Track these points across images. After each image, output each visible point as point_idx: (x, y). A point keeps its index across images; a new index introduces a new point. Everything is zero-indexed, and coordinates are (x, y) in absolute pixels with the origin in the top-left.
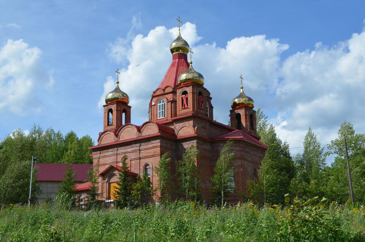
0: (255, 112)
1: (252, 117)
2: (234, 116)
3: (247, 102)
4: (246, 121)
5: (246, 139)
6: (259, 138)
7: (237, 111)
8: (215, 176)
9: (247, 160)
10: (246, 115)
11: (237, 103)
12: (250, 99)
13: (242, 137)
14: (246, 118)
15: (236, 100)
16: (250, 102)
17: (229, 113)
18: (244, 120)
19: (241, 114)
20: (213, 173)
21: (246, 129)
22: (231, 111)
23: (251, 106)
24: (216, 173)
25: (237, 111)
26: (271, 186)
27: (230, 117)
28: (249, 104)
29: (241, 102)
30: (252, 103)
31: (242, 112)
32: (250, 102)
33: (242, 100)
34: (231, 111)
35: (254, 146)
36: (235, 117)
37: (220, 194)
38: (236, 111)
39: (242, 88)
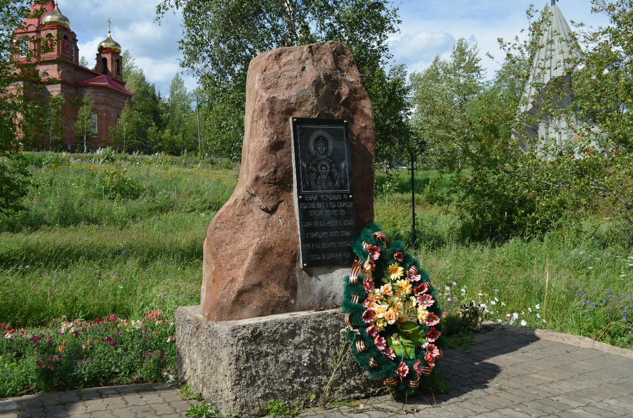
0: (121, 57)
1: (118, 61)
2: (100, 60)
3: (114, 47)
4: (112, 66)
5: (110, 86)
6: (123, 84)
7: (104, 56)
8: (79, 122)
9: (111, 106)
10: (112, 60)
11: (104, 47)
12: (117, 45)
13: (106, 83)
14: (112, 63)
15: (103, 44)
16: (116, 47)
17: (96, 56)
18: (110, 65)
19: (108, 59)
20: (76, 119)
21: (112, 74)
22: (97, 54)
23: (118, 51)
24: (79, 119)
25: (104, 56)
26: (129, 133)
27: (96, 61)
28: (116, 49)
29: (107, 47)
30: (119, 48)
31: (108, 57)
32: (116, 47)
33: (109, 45)
34: (97, 54)
35: (119, 93)
36: (101, 61)
37: (82, 138)
38: (102, 55)
39: (109, 32)
